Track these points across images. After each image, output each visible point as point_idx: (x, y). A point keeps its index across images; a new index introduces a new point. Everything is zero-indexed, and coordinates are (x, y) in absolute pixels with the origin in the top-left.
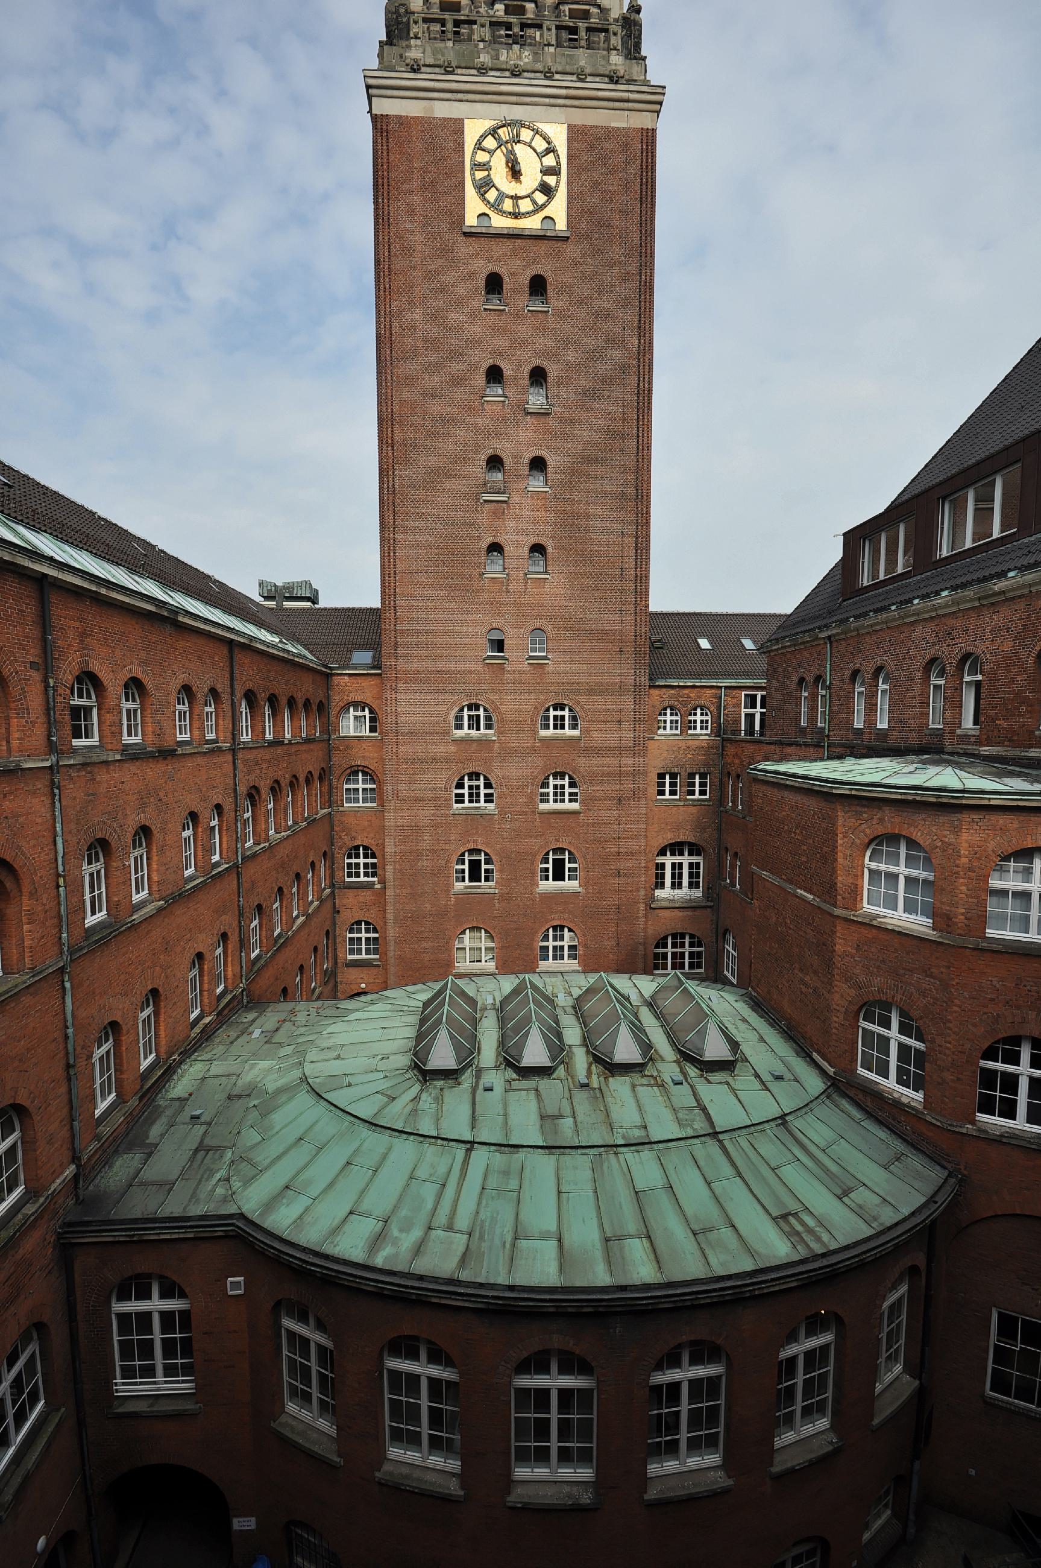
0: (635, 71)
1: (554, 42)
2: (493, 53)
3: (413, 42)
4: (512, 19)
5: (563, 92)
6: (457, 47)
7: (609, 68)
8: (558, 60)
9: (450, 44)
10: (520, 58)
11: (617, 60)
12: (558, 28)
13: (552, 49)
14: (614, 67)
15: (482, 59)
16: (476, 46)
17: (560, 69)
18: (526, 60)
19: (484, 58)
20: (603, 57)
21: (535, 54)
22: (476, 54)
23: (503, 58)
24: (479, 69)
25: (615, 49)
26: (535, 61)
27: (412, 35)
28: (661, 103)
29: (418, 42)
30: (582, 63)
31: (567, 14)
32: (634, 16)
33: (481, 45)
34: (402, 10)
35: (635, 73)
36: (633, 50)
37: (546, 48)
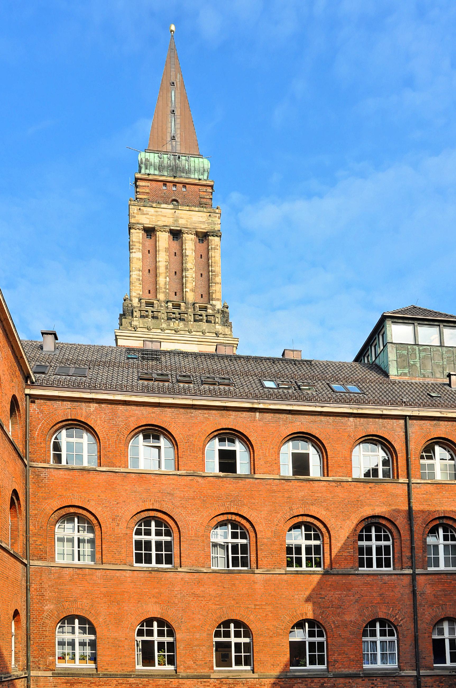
0: (227, 331)
1: (192, 320)
2: (167, 323)
3: (135, 319)
4: (176, 311)
5: (197, 340)
6: (153, 321)
7: (215, 330)
8: (194, 327)
9: (150, 320)
10: (179, 326)
11: (219, 328)
12: (194, 314)
13: (192, 323)
14: (217, 330)
15: (163, 326)
16: (161, 321)
17: (195, 330)
18: (181, 327)
19: (164, 326)
20: (213, 326)
21: (185, 324)
22: (160, 324)
23: (172, 325)
24: (161, 330)
25: (218, 323)
26: (185, 327)
27: (134, 316)
28: (237, 344)
29: (137, 319)
30: (204, 328)
31: (198, 307)
32: (225, 310)
33: (162, 321)
34: (130, 305)
35: (226, 331)
36: (226, 322)
37: (189, 322)
